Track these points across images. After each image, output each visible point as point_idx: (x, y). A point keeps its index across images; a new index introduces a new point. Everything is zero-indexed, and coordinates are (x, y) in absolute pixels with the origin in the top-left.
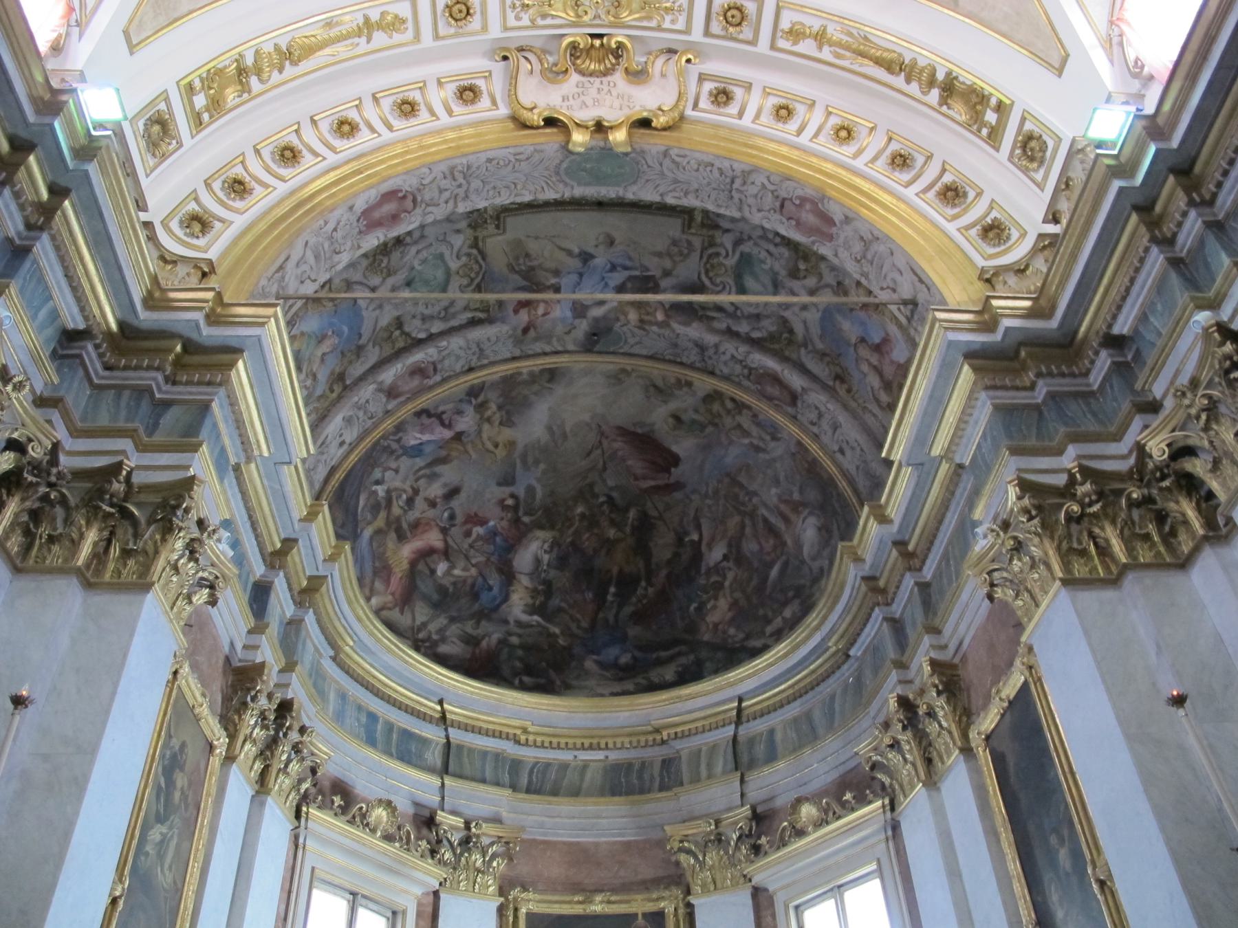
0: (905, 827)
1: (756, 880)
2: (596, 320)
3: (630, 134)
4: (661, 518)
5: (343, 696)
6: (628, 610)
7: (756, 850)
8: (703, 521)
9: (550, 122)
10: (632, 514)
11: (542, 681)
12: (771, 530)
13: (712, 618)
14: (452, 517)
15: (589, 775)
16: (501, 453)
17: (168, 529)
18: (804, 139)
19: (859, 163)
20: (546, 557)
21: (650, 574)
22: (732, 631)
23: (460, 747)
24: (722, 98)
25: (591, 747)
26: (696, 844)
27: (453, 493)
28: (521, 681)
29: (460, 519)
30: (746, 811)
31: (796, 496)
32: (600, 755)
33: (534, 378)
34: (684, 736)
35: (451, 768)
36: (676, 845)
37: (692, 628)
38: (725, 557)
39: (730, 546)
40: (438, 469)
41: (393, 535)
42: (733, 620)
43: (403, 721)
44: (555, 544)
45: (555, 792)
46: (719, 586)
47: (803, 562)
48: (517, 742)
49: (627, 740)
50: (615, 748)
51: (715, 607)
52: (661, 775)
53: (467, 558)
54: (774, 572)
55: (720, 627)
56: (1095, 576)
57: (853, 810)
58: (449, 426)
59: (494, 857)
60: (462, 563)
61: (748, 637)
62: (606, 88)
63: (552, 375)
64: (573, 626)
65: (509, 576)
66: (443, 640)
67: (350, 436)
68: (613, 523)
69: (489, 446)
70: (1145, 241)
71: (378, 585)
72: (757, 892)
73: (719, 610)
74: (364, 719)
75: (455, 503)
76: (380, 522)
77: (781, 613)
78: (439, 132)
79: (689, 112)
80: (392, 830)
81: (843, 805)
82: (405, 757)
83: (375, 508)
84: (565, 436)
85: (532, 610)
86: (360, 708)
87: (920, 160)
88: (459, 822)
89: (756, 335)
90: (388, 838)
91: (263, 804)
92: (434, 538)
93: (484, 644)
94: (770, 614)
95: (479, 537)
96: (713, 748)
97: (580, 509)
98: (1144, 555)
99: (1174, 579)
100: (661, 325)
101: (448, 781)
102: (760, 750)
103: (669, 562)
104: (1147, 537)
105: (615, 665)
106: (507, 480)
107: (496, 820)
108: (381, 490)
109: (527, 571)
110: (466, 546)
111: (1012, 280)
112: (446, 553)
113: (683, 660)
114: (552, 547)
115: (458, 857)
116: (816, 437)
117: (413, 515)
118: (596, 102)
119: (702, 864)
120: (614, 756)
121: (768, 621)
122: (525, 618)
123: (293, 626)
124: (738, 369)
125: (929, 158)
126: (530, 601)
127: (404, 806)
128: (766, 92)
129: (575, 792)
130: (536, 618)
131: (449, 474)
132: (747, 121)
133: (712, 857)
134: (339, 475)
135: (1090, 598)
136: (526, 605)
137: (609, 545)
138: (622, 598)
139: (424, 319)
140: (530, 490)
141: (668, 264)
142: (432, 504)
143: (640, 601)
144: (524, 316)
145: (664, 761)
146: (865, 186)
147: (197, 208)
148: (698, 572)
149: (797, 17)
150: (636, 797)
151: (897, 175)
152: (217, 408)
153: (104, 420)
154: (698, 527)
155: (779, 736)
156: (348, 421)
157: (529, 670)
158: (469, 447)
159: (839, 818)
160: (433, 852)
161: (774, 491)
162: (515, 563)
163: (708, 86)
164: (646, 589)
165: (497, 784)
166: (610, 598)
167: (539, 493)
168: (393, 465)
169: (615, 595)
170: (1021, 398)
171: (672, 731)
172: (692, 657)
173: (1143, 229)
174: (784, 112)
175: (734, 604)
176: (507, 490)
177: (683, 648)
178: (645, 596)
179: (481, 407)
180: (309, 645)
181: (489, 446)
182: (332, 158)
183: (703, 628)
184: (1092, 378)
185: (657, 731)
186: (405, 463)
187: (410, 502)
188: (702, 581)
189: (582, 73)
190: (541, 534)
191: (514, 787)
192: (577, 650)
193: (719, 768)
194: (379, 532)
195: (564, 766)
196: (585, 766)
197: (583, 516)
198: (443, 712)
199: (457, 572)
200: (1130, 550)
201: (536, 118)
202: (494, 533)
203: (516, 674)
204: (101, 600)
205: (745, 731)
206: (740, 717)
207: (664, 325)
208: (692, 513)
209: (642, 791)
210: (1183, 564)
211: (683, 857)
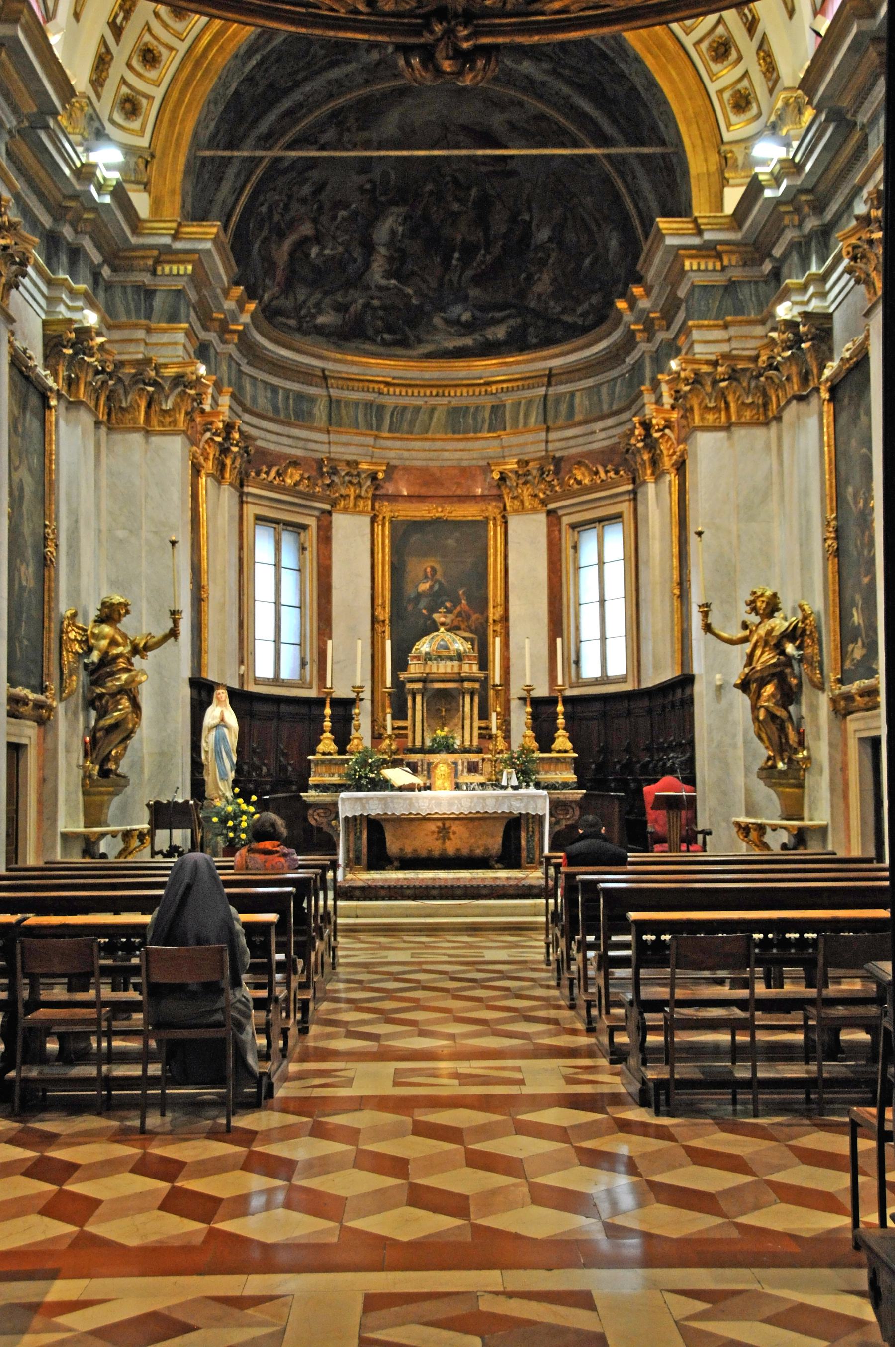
1: (552, 506)
4: (499, 196)
6: (470, 273)
8: (533, 205)
10: (474, 192)
11: (398, 337)
12: (588, 230)
13: (538, 288)
14: (320, 208)
20: (400, 229)
21: (488, 244)
22: (552, 303)
23: (338, 401)
27: (319, 189)
28: (382, 339)
29: (327, 205)
32: (445, 400)
33: (384, 96)
35: (333, 421)
37: (522, 294)
38: (551, 239)
39: (553, 230)
40: (306, 175)
42: (553, 293)
44: (407, 218)
46: (543, 263)
47: (608, 264)
51: (539, 279)
52: (491, 419)
53: (334, 238)
54: (587, 262)
55: (543, 298)
56: (717, 424)
61: (563, 312)
63: (402, 92)
64: (424, 286)
65: (369, 247)
66: (320, 312)
68: (458, 200)
71: (268, 282)
72: (550, 513)
73: (543, 284)
75: (322, 197)
77: (589, 299)
84: (413, 131)
85: (388, 275)
92: (307, 229)
93: (352, 309)
94: (581, 297)
95: (344, 219)
96: (530, 402)
97: (429, 187)
103: (505, 236)
105: (458, 322)
108: (264, 209)
109: (383, 241)
110: (333, 228)
112: (318, 238)
113: (512, 322)
114: (405, 218)
116: (622, 175)
120: (455, 402)
121: (579, 302)
122: (384, 282)
126: (387, 267)
130: (393, 282)
134: (235, 218)
136: (385, 271)
137: (456, 215)
138: (466, 262)
142: (304, 201)
143: (479, 266)
144: (375, 56)
145: (493, 406)
147: (129, 92)
148: (528, 246)
154: (529, 209)
155: (577, 400)
157: (390, 329)
162: (374, 236)
164: (484, 256)
166: (454, 262)
168: (272, 186)
169: (459, 260)
171: (500, 386)
172: (519, 320)
175: (554, 280)
176: (363, 178)
177: (513, 311)
178: (483, 262)
179: (340, 124)
183: (530, 296)
184: (763, 267)
185: (488, 384)
186: (281, 182)
187: (287, 207)
188: (531, 255)
190: (396, 210)
192: (428, 308)
194: (266, 240)
197: (431, 193)
199: (327, 252)
202: (355, 214)
203: (378, 332)
205: (552, 390)
208: (524, 197)
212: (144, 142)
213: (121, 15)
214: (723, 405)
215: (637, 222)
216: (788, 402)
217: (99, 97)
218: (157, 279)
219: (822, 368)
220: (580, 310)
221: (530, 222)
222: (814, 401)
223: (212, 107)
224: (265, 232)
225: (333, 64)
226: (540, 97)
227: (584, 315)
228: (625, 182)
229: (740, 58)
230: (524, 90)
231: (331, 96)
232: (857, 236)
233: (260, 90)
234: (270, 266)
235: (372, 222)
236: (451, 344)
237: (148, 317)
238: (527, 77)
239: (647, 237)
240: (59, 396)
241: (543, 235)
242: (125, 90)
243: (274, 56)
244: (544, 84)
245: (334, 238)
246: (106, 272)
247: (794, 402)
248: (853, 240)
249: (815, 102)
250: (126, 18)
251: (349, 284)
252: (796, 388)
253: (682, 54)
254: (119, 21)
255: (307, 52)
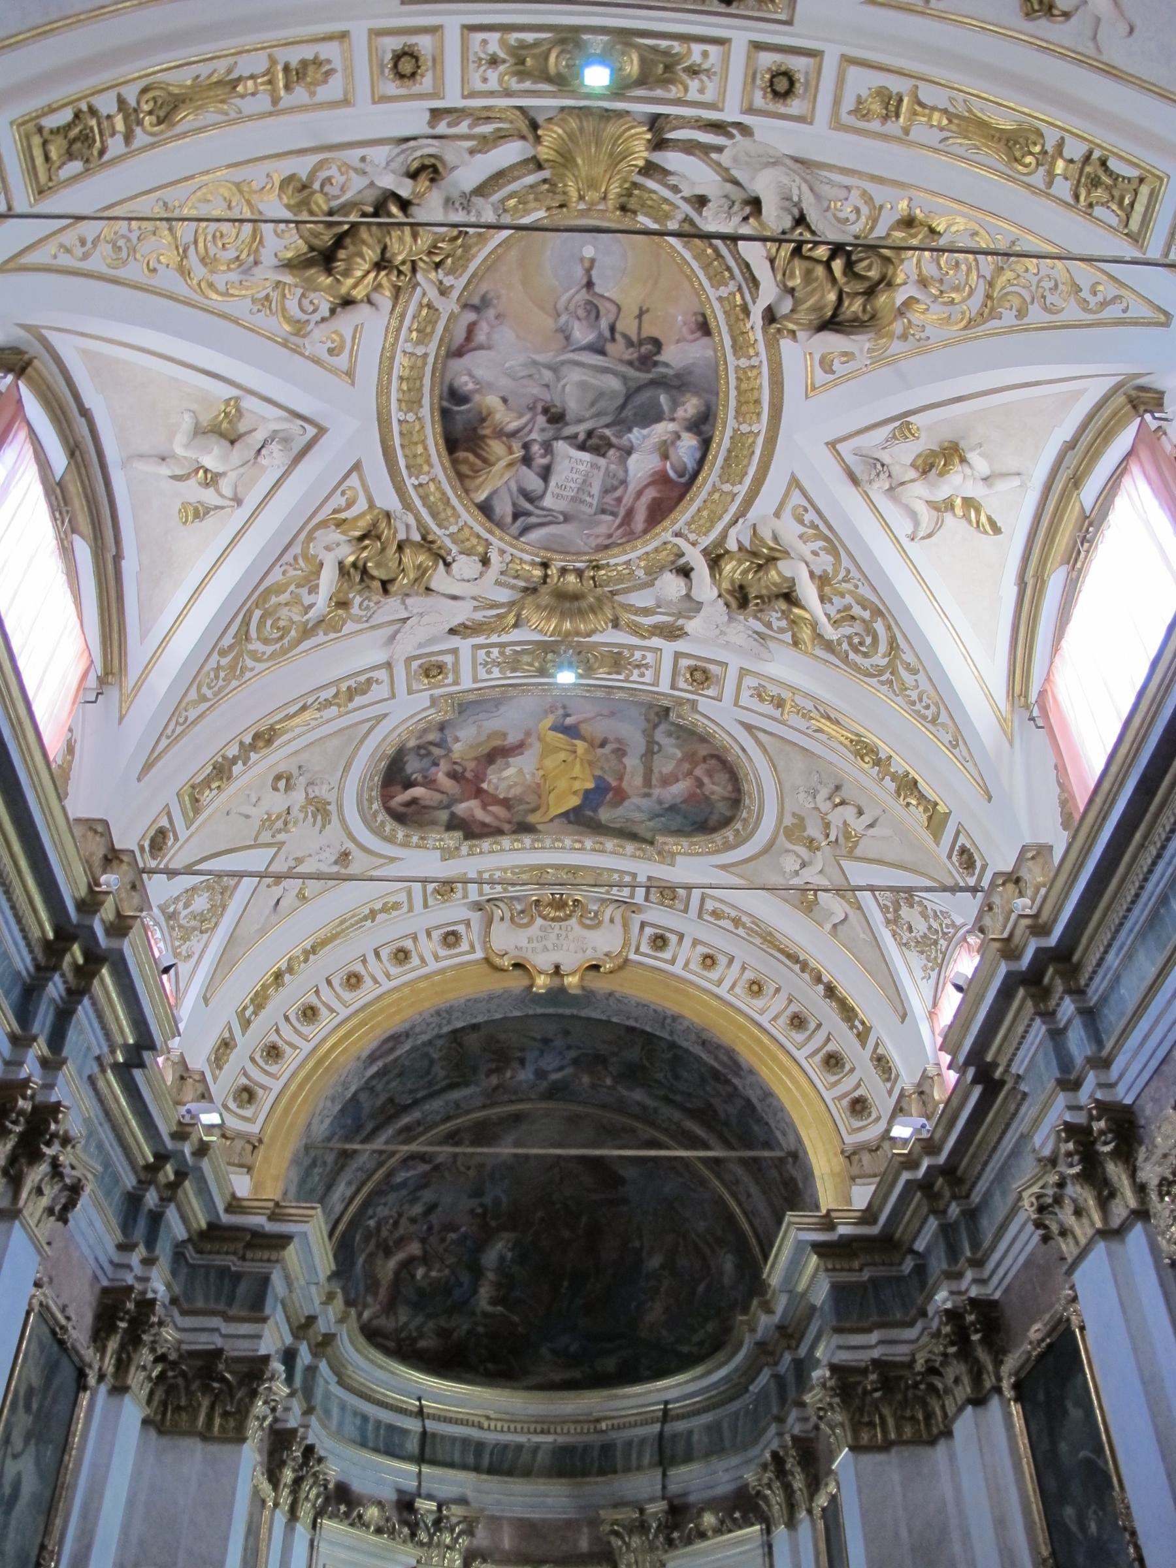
0: (775, 1549)
2: (555, 1082)
3: (582, 979)
5: (343, 1407)
7: (670, 1543)
9: (517, 966)
10: (584, 1220)
14: (430, 1228)
15: (540, 1456)
16: (472, 1173)
17: (254, 1394)
18: (722, 991)
19: (764, 1020)
20: (509, 1255)
22: (664, 1333)
23: (434, 1435)
24: (659, 943)
25: (542, 1432)
26: (624, 1527)
28: (486, 1369)
29: (436, 1229)
30: (662, 1505)
31: (719, 1233)
32: (549, 1439)
34: (619, 1428)
36: (608, 1528)
38: (663, 1267)
40: (419, 1194)
41: (381, 1254)
43: (387, 1417)
45: (510, 1473)
48: (480, 1427)
49: (572, 1427)
50: (562, 1433)
53: (442, 1260)
54: (701, 1288)
57: (741, 1528)
58: (429, 1162)
59: (460, 1535)
60: (437, 1266)
62: (564, 934)
63: (517, 1119)
65: (477, 1272)
66: (421, 1335)
67: (348, 1194)
69: (463, 1169)
70: (925, 1210)
71: (370, 1299)
73: (655, 1313)
74: (358, 1422)
75: (434, 1218)
76: (372, 1246)
78: (427, 977)
79: (633, 956)
80: (382, 1523)
81: (735, 1520)
82: (391, 1451)
83: (367, 1238)
86: (355, 1413)
87: (812, 1026)
88: (433, 1506)
89: (688, 1105)
90: (379, 1531)
91: (293, 1529)
92: (415, 1248)
93: (455, 1335)
95: (453, 1242)
96: (643, 1441)
97: (539, 1214)
98: (908, 1432)
99: (925, 1452)
100: (608, 1087)
101: (426, 1469)
102: (681, 1446)
104: (913, 1418)
106: (477, 1193)
107: (462, 1501)
108: (372, 1223)
110: (441, 1250)
111: (866, 1157)
112: (425, 1259)
115: (431, 1536)
116: (734, 1195)
117: (401, 1231)
118: (556, 947)
119: (628, 1545)
120: (561, 1440)
122: (489, 1309)
123: (311, 1370)
124: (674, 1127)
125: (819, 1026)
127: (390, 1495)
128: (696, 942)
129: (527, 1473)
130: (500, 1308)
131: (428, 1195)
132: (677, 969)
133: (636, 1542)
134: (341, 1227)
135: (867, 1459)
139: (411, 1092)
140: (497, 1202)
141: (615, 1049)
142: (413, 1221)
146: (766, 1040)
149: (717, 905)
150: (579, 1480)
151: (793, 1034)
152: (277, 1280)
153: (200, 1304)
154: (640, 1237)
155: (695, 1437)
156: (349, 1183)
158: (447, 1174)
159: (730, 1531)
160: (413, 1535)
161: (702, 1223)
163: (649, 931)
165: (464, 1467)
166: (563, 1290)
167: (504, 1199)
170: (853, 1278)
171: (610, 1423)
173: (925, 1201)
174: (709, 961)
180: (321, 1381)
181: (463, 1169)
182: (344, 1012)
185: (598, 1421)
186: (392, 1198)
187: (396, 1224)
189: (544, 918)
190: (506, 1235)
191: (477, 1469)
193: (646, 1460)
194: (371, 1255)
195: (520, 1447)
196: (536, 1448)
198: (421, 1407)
199: (434, 1274)
200: (899, 1429)
201: (506, 963)
202: (464, 1238)
204: (214, 1448)
206: (666, 1417)
207: (613, 1088)
209: (584, 1474)
210: (932, 1442)
211: (613, 1539)
212: (254, 1129)
213: (251, 1009)
214: (877, 1421)
215: (753, 1241)
216: (961, 1409)
217: (215, 1078)
218: (247, 1264)
219: (998, 1363)
220: (696, 1338)
221: (641, 1248)
222: (995, 1403)
223: (329, 1103)
224: (372, 1246)
225: (453, 1086)
226: (652, 1124)
227: (701, 1343)
228: (740, 1204)
229: (852, 1070)
230: (635, 1117)
231: (448, 1118)
232: (1040, 1183)
233: (379, 1102)
234: (373, 1285)
235: (480, 1247)
236: (557, 1377)
237: (230, 1302)
238: (638, 1103)
239: (766, 1258)
240: (101, 1378)
241: (654, 1262)
242: (244, 1081)
243: (396, 1071)
244: (656, 1110)
245: (442, 1260)
246: (190, 1252)
247: (970, 1408)
248: (1036, 1189)
249: (961, 1059)
250: (255, 1013)
251: (452, 1310)
252: (969, 1390)
253: (796, 1067)
254: (248, 1013)
255: (428, 1072)
